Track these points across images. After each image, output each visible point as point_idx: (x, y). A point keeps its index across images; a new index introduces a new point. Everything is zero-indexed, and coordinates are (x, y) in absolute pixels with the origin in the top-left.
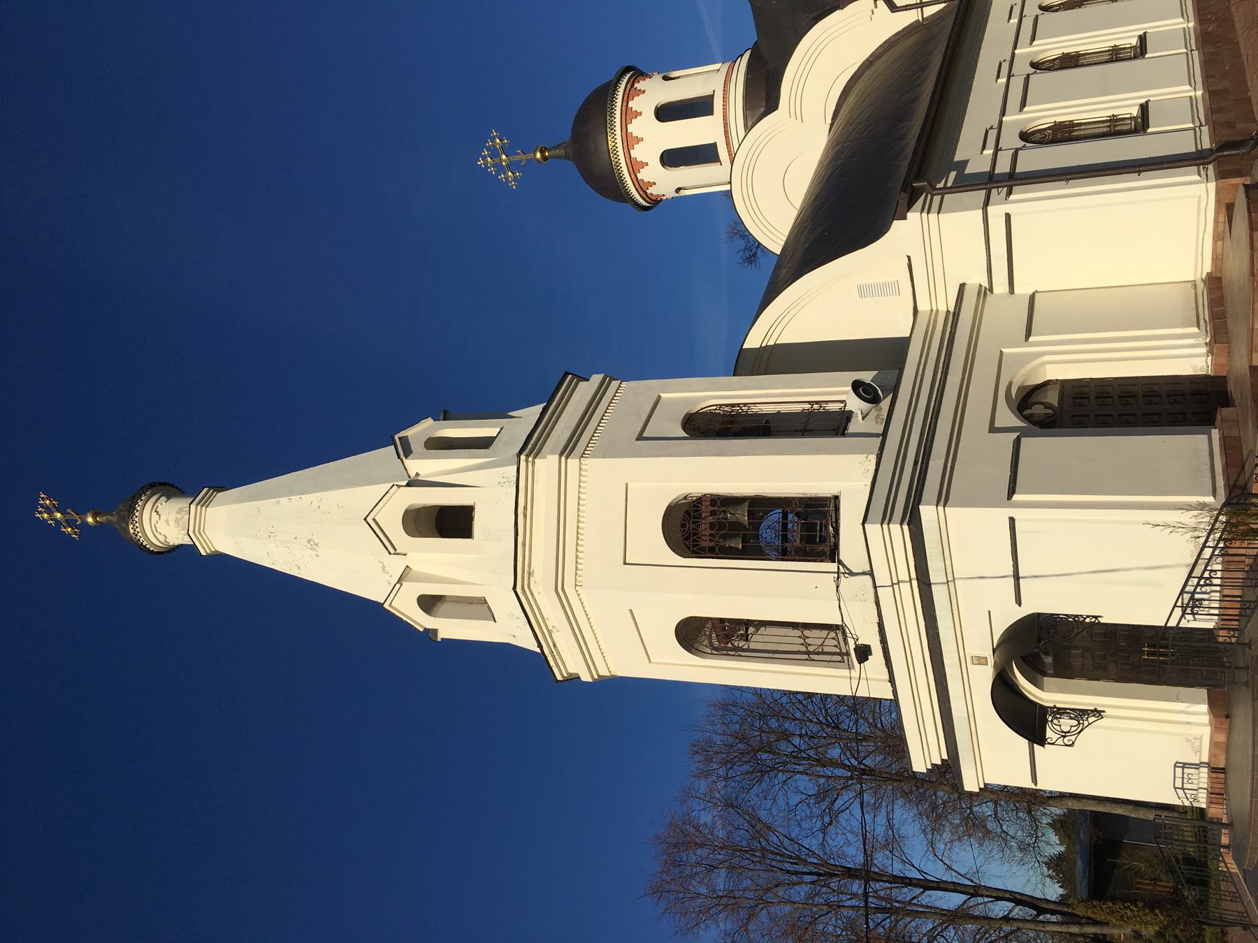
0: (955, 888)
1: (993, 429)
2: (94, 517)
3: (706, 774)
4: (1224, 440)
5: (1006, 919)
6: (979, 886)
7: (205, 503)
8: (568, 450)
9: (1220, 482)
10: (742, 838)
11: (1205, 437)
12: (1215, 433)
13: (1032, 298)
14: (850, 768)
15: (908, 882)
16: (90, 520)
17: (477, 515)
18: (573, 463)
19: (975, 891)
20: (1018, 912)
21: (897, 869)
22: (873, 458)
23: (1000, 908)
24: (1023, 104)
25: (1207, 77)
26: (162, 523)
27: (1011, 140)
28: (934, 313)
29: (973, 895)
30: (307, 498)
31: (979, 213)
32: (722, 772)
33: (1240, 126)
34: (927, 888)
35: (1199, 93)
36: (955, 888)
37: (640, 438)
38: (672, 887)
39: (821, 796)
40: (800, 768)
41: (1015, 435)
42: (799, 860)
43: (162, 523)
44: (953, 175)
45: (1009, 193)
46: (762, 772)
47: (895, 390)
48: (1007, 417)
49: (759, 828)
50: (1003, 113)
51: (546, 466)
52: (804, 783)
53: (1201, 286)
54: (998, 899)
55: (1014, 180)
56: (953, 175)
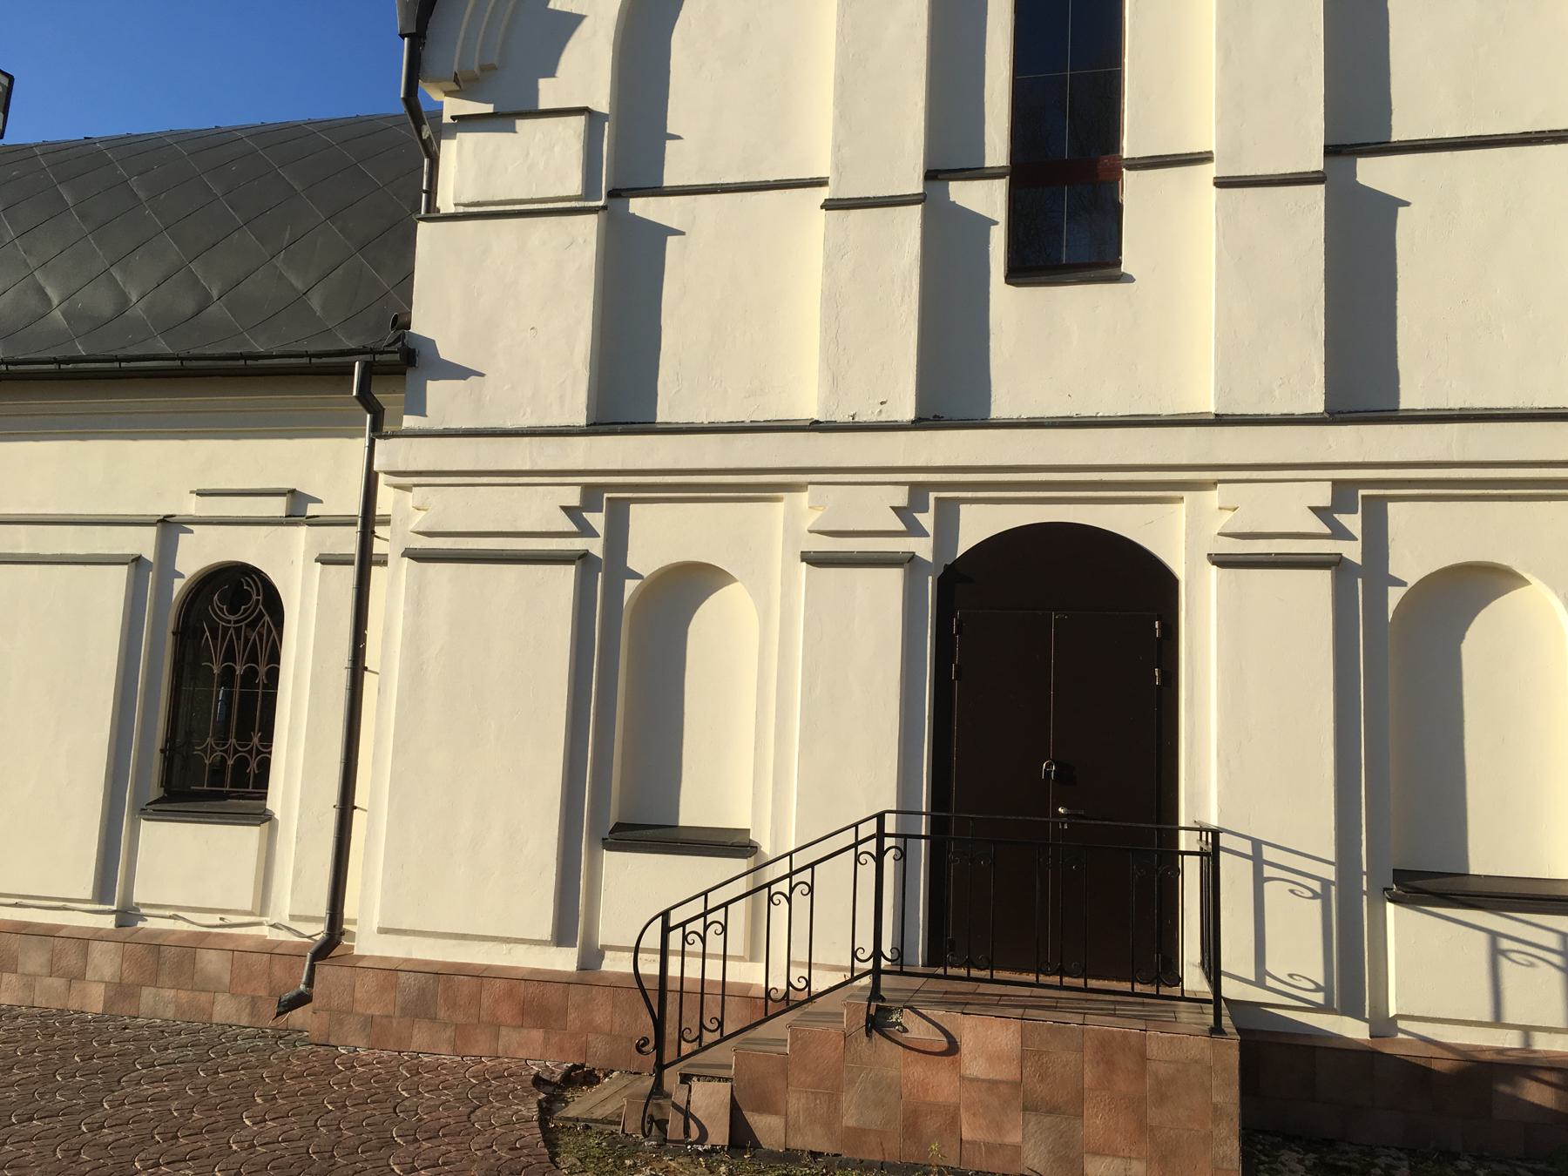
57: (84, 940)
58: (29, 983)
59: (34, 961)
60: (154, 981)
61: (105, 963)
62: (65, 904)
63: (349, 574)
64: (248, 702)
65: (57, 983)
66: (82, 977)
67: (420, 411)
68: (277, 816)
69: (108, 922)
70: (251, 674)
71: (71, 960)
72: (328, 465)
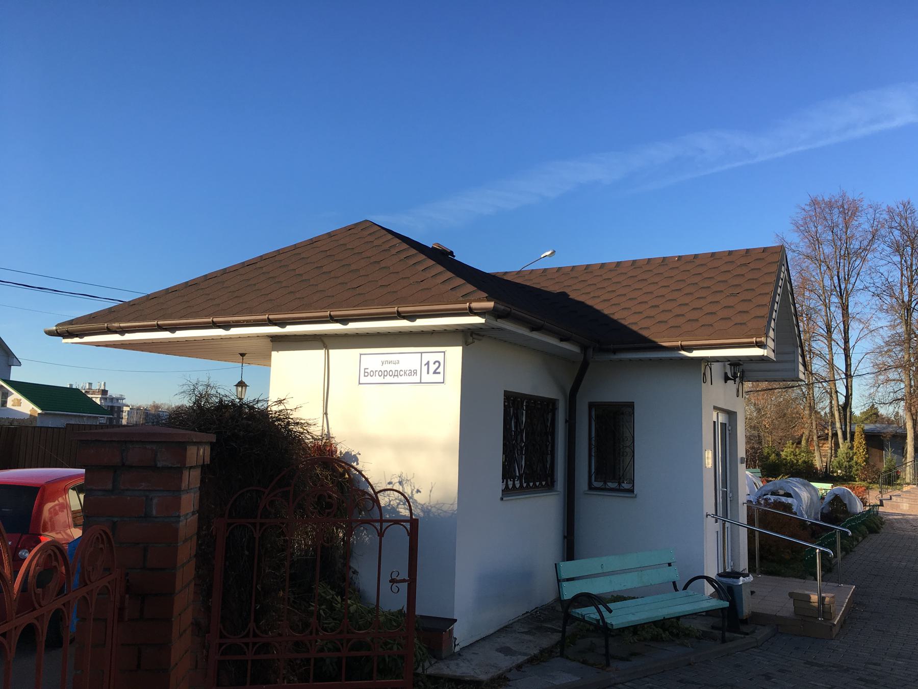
0: (848, 366)
3: (892, 218)
5: (837, 392)
6: (851, 377)
10: (855, 245)
14: (910, 301)
15: (846, 341)
19: (848, 376)
20: (842, 400)
21: (853, 335)
23: (842, 389)
29: (846, 374)
32: (894, 224)
34: (844, 349)
36: (848, 366)
38: (818, 210)
39: (890, 287)
40: (905, 272)
42: (847, 280)
46: (898, 249)
49: (862, 253)
52: (895, 276)
54: (847, 387)
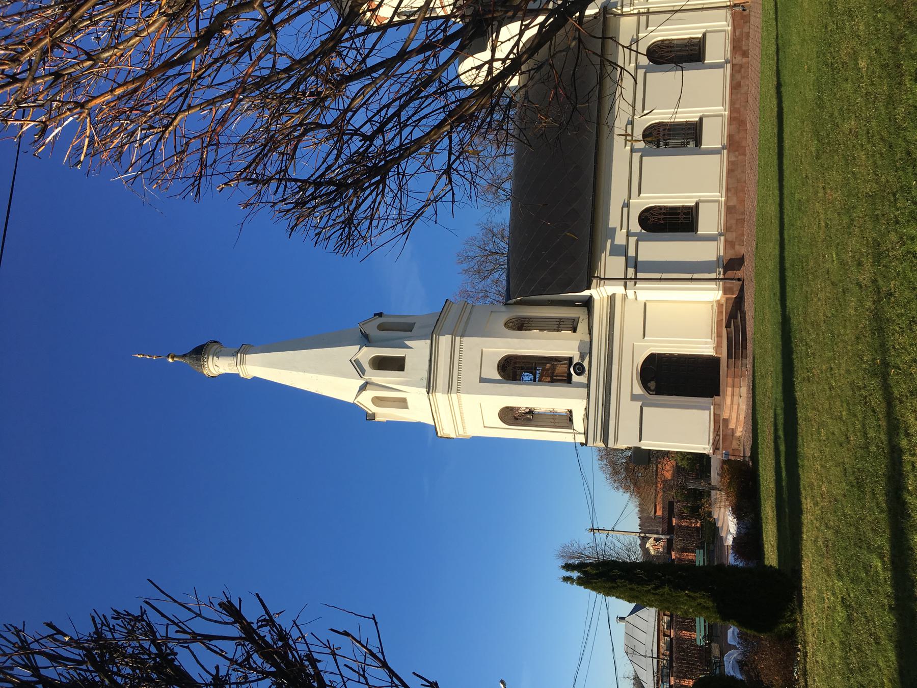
1: (634, 398)
2: (173, 358)
4: (715, 414)
7: (242, 362)
8: (450, 389)
9: (712, 437)
11: (708, 412)
12: (712, 407)
13: (645, 304)
16: (170, 360)
17: (408, 401)
18: (454, 396)
22: (585, 401)
24: (640, 193)
25: (728, 190)
26: (217, 366)
27: (636, 227)
28: (602, 299)
30: (308, 375)
31: (623, 288)
33: (737, 247)
35: (723, 199)
37: (482, 380)
41: (640, 403)
43: (217, 366)
44: (609, 241)
45: (635, 284)
47: (590, 353)
48: (638, 390)
50: (630, 197)
51: (440, 398)
53: (715, 304)
55: (637, 272)
56: (609, 241)
57: (733, 66)
58: (743, 77)
59: (738, 77)
60: (740, 48)
61: (739, 59)
62: (725, 76)
63: (651, 17)
64: (671, 214)
65: (743, 70)
66: (741, 66)
67: (617, 2)
68: (704, 30)
69: (729, 65)
70: (664, 214)
71: (737, 68)
72: (626, 28)
